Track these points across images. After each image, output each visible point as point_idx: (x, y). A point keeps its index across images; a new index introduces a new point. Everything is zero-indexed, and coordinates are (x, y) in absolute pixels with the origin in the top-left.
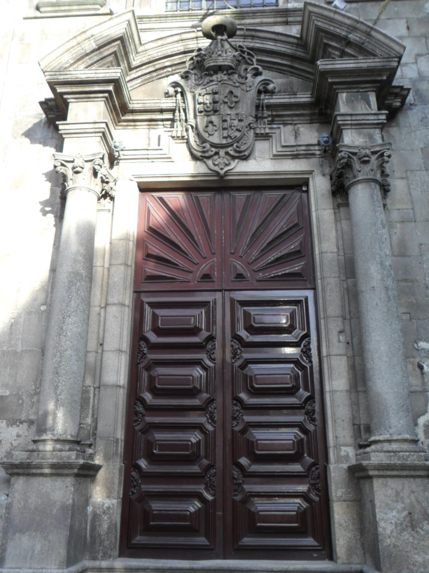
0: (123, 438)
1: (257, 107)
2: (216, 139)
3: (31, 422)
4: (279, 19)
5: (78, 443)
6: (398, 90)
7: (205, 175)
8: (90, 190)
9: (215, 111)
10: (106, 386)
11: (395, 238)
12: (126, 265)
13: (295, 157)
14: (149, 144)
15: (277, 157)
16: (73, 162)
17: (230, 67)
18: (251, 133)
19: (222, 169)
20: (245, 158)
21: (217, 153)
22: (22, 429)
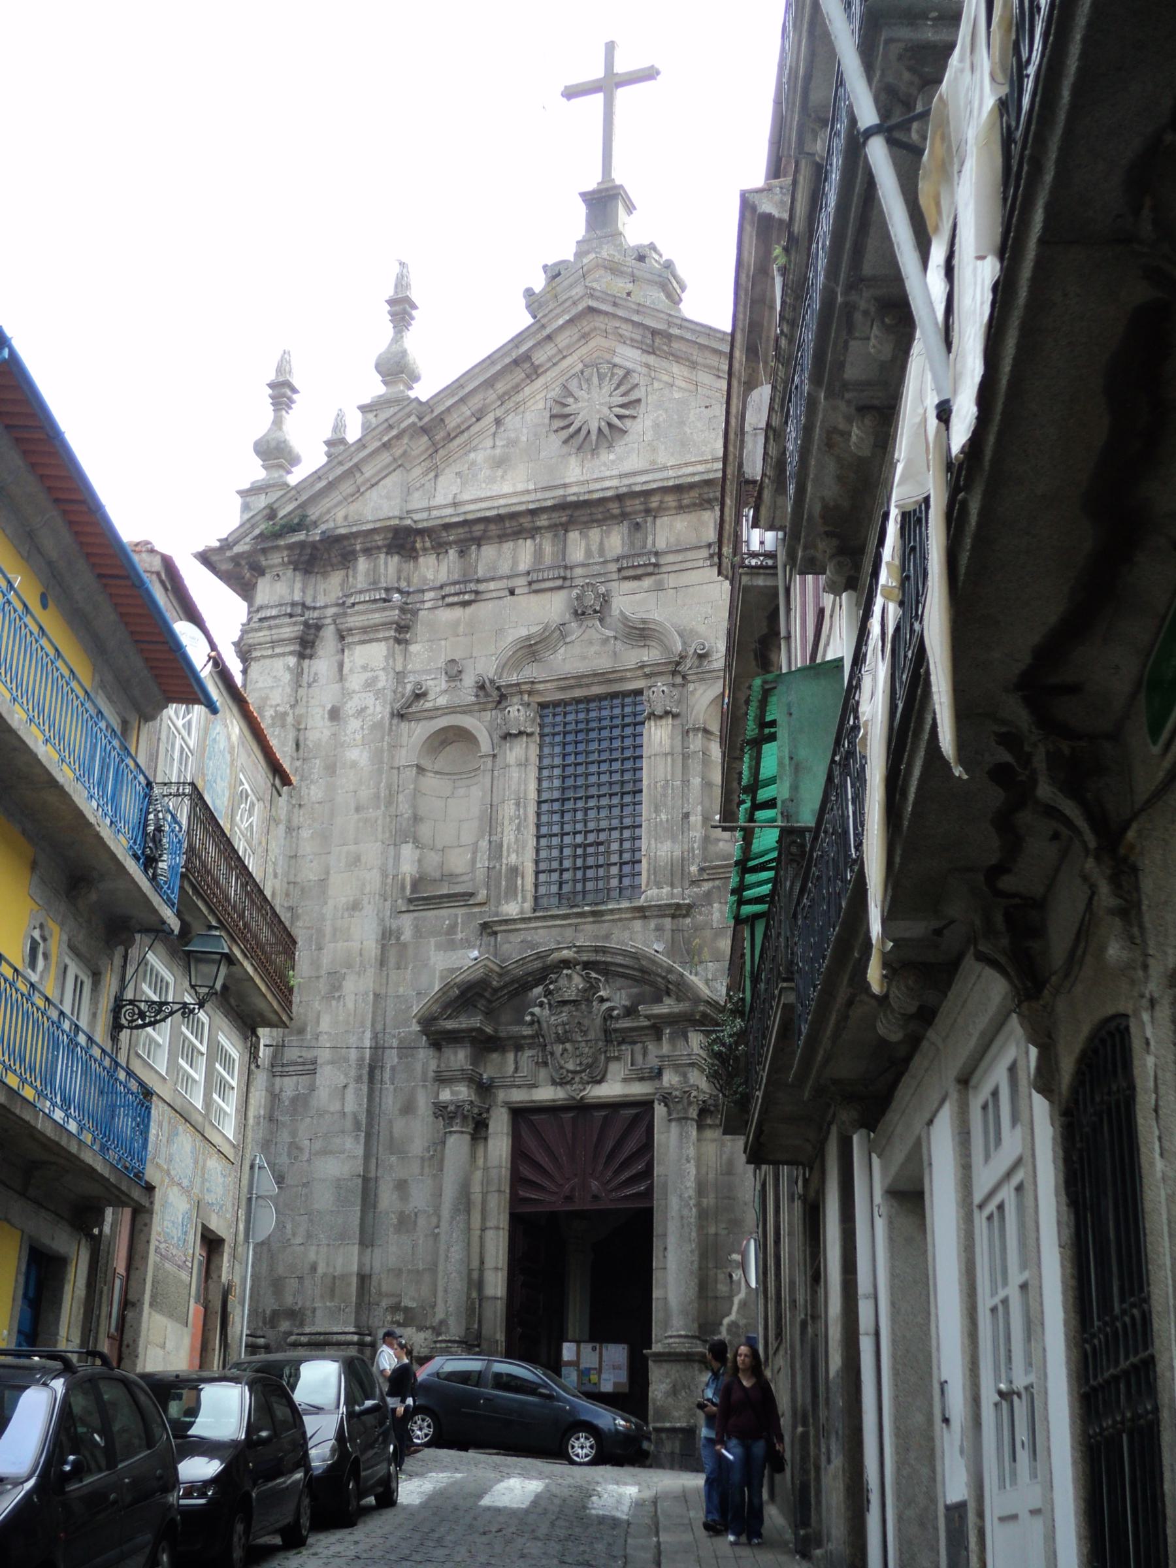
0: (503, 1339)
1: (605, 1031)
3: (433, 1328)
5: (466, 1343)
7: (565, 1099)
8: (462, 1132)
9: (568, 1041)
10: (488, 1298)
11: (724, 1157)
12: (499, 1191)
13: (641, 1079)
14: (516, 1070)
15: (625, 1080)
16: (446, 1107)
17: (574, 1001)
18: (603, 1057)
20: (600, 1082)
22: (428, 1334)
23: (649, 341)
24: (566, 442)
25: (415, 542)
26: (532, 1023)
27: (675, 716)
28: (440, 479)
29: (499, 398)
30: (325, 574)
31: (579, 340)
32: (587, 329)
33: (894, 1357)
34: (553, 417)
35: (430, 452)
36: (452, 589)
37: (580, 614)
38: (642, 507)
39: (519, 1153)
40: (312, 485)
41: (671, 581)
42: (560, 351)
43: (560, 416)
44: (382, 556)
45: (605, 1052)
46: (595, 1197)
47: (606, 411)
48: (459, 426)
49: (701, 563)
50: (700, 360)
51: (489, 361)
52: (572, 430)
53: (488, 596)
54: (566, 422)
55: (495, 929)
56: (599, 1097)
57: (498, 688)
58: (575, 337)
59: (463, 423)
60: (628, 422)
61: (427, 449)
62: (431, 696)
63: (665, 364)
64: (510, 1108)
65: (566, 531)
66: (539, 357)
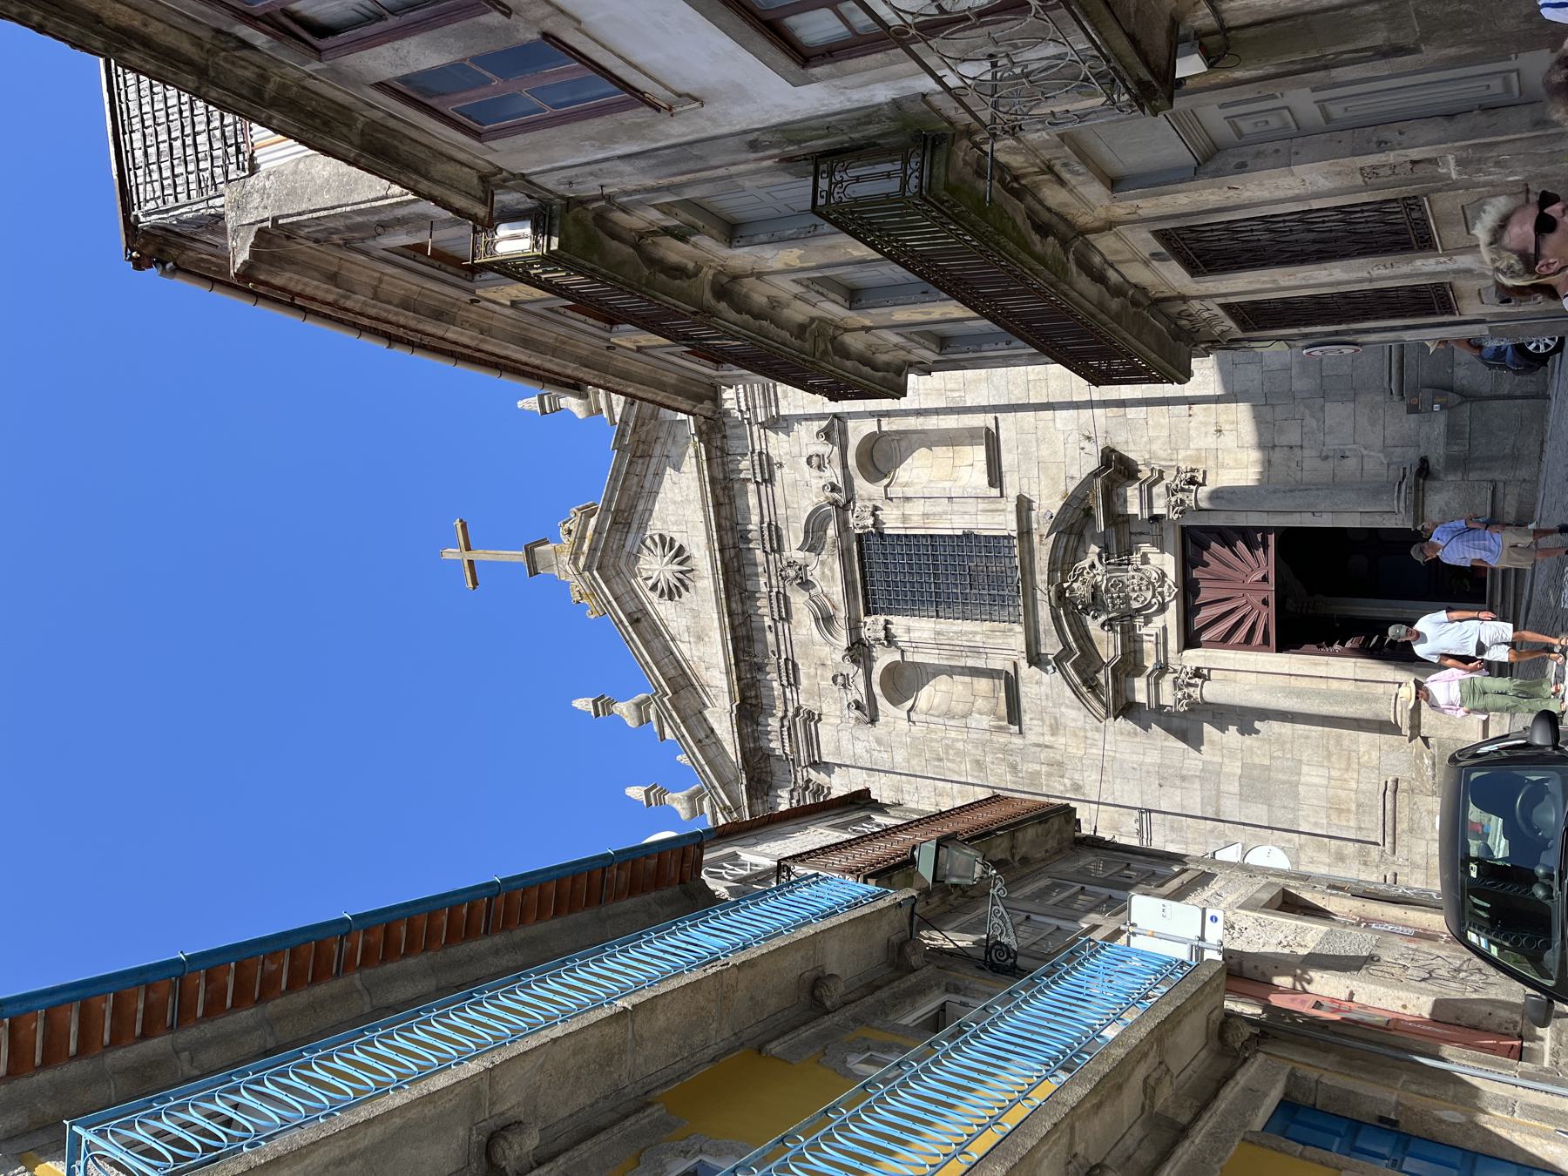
2: (1149, 594)
4: (1026, 539)
21: (1160, 593)
23: (621, 526)
24: (687, 589)
27: (876, 508)
28: (711, 684)
29: (657, 637)
30: (772, 773)
33: (1421, 316)
34: (671, 599)
36: (784, 678)
37: (806, 584)
38: (730, 534)
39: (1224, 641)
41: (781, 511)
42: (627, 592)
43: (671, 594)
44: (760, 728)
46: (1265, 579)
47: (667, 559)
48: (675, 668)
49: (769, 489)
50: (634, 489)
52: (678, 585)
53: (789, 650)
54: (674, 589)
55: (1034, 654)
57: (853, 644)
58: (618, 580)
60: (677, 545)
61: (691, 693)
62: (858, 697)
63: (637, 516)
65: (746, 591)
66: (631, 607)
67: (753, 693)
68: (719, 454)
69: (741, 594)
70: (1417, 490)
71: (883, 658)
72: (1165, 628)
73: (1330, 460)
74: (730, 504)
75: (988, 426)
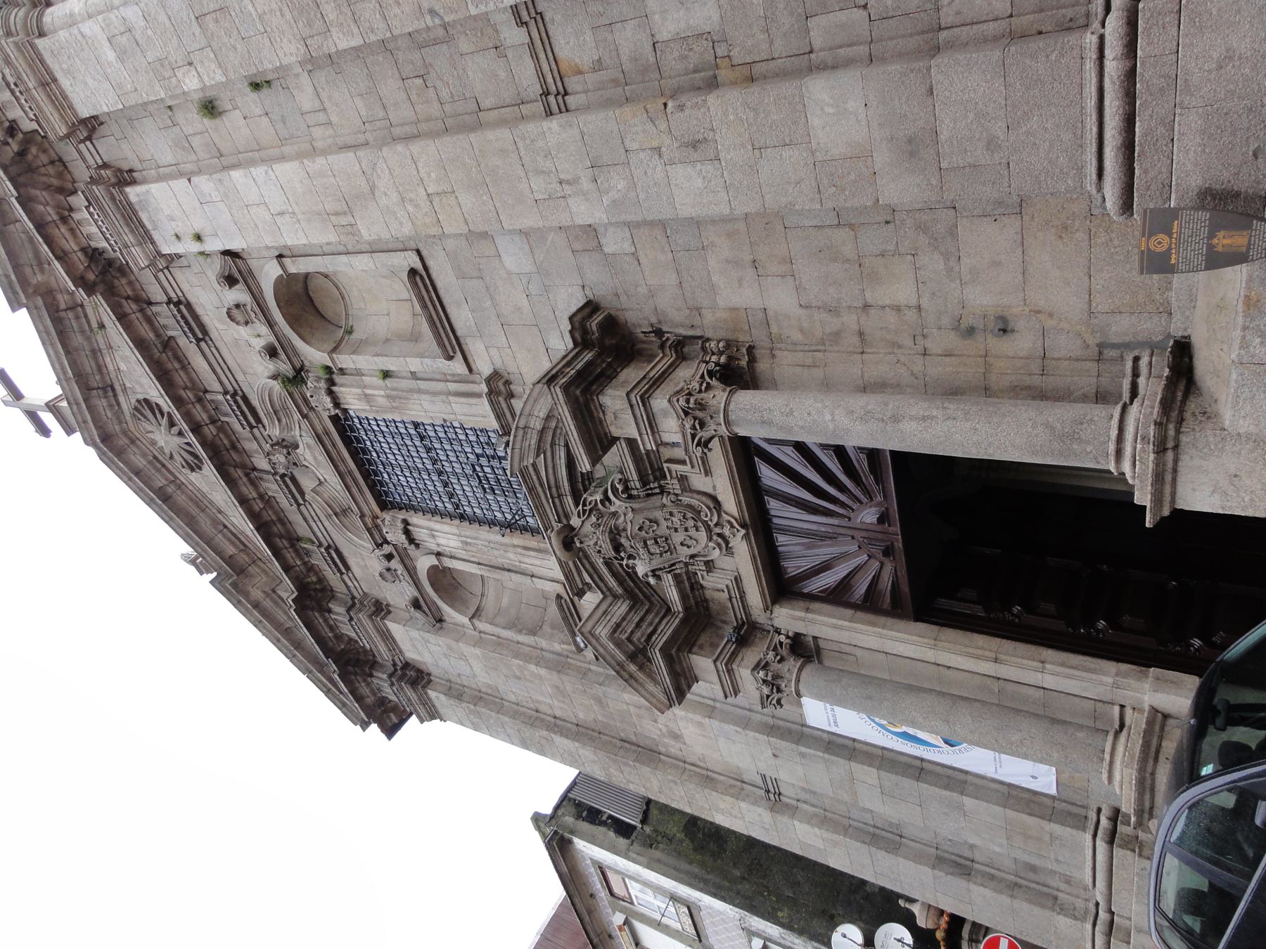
6: (577, 335)
19: (738, 531)
21: (719, 535)
25: (315, 590)
26: (658, 578)
31: (138, 447)
32: (127, 442)
35: (261, 564)
38: (198, 406)
40: (301, 662)
45: (677, 495)
46: (883, 519)
51: (170, 522)
56: (739, 504)
59: (229, 540)
64: (774, 602)
67: (314, 579)
68: (134, 307)
69: (247, 475)
70: (1161, 449)
71: (424, 563)
72: (738, 580)
73: (980, 337)
74: (184, 368)
75: (413, 265)
